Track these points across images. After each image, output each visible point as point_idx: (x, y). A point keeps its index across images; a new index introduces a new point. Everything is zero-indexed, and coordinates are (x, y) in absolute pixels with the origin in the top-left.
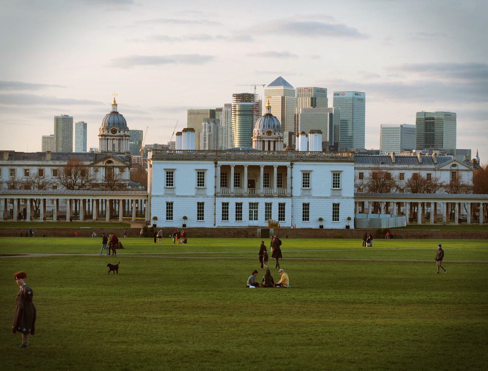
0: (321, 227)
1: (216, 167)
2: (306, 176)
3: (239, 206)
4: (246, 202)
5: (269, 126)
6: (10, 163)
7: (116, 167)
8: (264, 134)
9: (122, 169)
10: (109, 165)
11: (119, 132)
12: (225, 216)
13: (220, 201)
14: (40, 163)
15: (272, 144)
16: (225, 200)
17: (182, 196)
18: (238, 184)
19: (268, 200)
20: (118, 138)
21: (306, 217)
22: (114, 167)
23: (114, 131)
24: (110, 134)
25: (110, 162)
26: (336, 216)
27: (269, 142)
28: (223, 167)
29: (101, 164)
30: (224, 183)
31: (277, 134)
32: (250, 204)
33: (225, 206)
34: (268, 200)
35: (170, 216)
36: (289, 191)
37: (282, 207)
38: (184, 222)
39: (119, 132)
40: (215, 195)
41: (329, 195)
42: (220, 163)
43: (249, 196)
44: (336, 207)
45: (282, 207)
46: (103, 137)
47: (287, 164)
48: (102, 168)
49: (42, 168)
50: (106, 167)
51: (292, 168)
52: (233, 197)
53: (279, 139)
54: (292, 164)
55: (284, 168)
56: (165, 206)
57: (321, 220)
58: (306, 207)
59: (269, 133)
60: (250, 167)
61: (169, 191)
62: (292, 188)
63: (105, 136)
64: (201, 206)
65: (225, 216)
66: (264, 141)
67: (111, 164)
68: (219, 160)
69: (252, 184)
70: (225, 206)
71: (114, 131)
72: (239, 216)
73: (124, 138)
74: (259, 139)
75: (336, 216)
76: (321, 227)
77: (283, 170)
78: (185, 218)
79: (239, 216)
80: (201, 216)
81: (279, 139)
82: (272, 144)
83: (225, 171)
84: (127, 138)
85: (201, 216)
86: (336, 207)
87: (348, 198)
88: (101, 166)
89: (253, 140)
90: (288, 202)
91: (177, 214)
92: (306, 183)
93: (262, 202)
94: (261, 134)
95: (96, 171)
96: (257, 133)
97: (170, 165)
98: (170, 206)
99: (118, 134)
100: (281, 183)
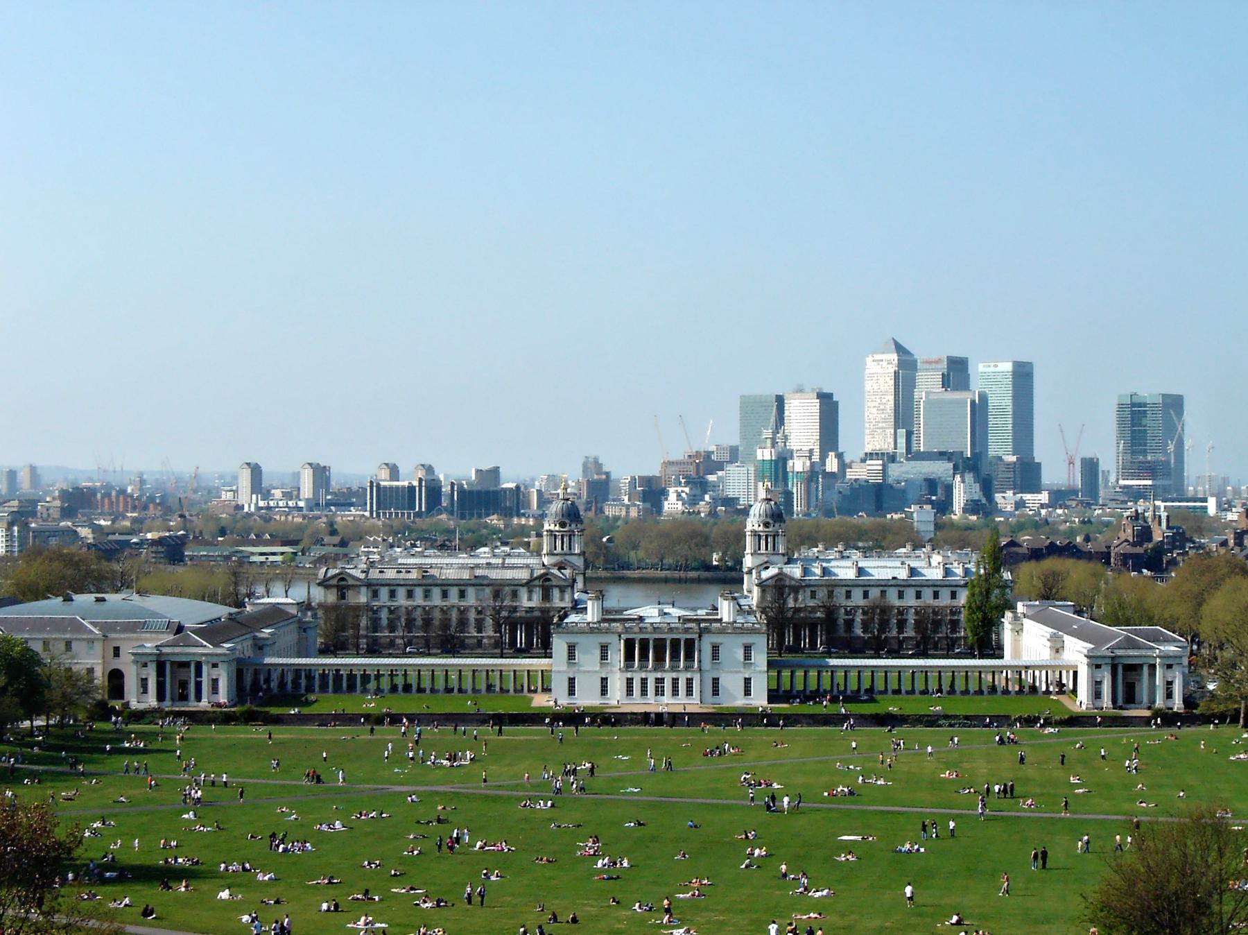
2: (715, 649)
3: (644, 682)
9: (562, 590)
16: (629, 675)
18: (644, 656)
19: (674, 675)
22: (552, 586)
23: (563, 525)
24: (557, 528)
25: (549, 580)
26: (747, 692)
29: (536, 582)
30: (629, 656)
33: (630, 682)
34: (674, 675)
35: (571, 692)
37: (689, 682)
44: (747, 681)
45: (689, 682)
55: (693, 640)
59: (766, 525)
65: (630, 691)
69: (659, 658)
70: (630, 682)
75: (747, 692)
77: (690, 644)
80: (604, 691)
83: (629, 645)
85: (604, 691)
86: (747, 681)
93: (668, 678)
95: (530, 592)
97: (572, 639)
98: (572, 682)
100: (689, 656)
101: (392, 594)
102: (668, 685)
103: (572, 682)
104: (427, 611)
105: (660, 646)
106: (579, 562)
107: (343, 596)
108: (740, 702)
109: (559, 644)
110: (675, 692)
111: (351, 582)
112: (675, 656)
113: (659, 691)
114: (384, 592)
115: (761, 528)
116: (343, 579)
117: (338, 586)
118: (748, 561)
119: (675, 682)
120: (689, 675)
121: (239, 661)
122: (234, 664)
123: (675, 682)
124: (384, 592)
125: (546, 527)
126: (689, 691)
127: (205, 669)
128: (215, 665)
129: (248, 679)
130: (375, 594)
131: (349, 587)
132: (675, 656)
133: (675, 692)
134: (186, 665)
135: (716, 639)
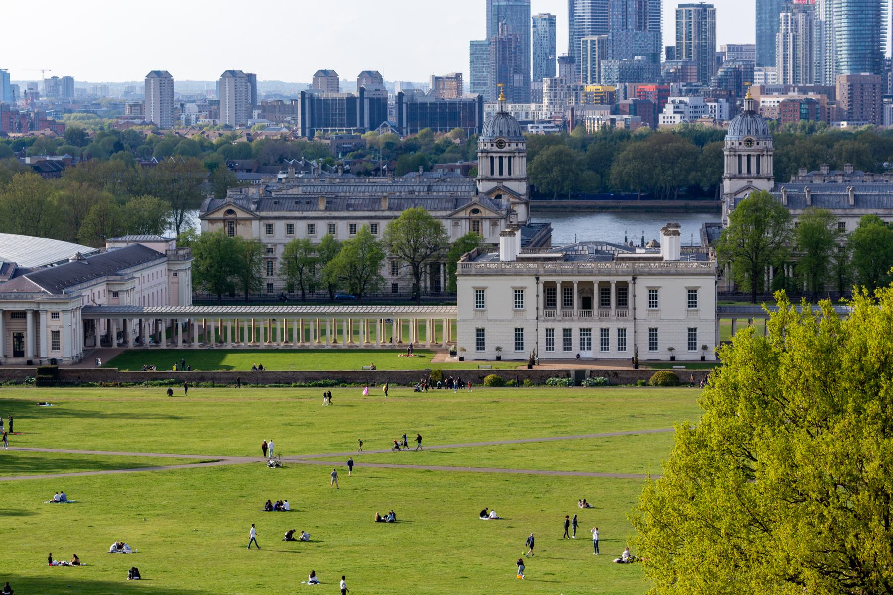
0: (673, 358)
1: (537, 283)
3: (567, 332)
4: (576, 327)
5: (749, 131)
6: (327, 214)
7: (486, 218)
8: (740, 144)
9: (494, 222)
10: (475, 215)
11: (509, 145)
12: (550, 345)
13: (543, 326)
14: (372, 214)
15: (753, 160)
16: (550, 325)
17: (496, 321)
18: (568, 302)
20: (508, 155)
21: (653, 345)
22: (482, 219)
24: (495, 148)
25: (476, 211)
27: (749, 157)
28: (546, 284)
29: (462, 214)
30: (550, 302)
31: (761, 144)
32: (581, 330)
33: (550, 332)
35: (480, 344)
36: (630, 312)
37: (622, 332)
38: (496, 353)
39: (509, 145)
40: (537, 319)
41: (682, 317)
42: (543, 279)
43: (579, 320)
44: (692, 332)
45: (622, 332)
46: (484, 154)
47: (629, 279)
48: (464, 221)
49: (374, 221)
50: (469, 218)
51: (634, 283)
52: (559, 321)
53: (765, 153)
54: (634, 279)
55: (625, 284)
56: (475, 333)
57: (671, 349)
58: (653, 332)
59: (749, 142)
60: (580, 283)
61: (479, 315)
62: (635, 309)
63: (487, 152)
64: (519, 332)
65: (550, 345)
66: (740, 156)
67: (478, 215)
68: (542, 275)
69: (587, 304)
70: (550, 332)
71: (500, 144)
72: (567, 346)
73: (517, 154)
74: (732, 153)
75: (692, 345)
76: (673, 358)
77: (623, 289)
78: (498, 349)
79: (567, 346)
80: (519, 345)
81: (765, 153)
82: (753, 160)
83: (549, 289)
84: (521, 154)
85: (519, 345)
86: (692, 332)
87: (707, 321)
88: (462, 218)
89: (726, 153)
90: (629, 327)
91: (490, 342)
92: (653, 300)
93: (596, 329)
94: (736, 144)
95: (456, 224)
96: (729, 143)
97: (480, 282)
98: (480, 333)
99: (507, 148)
100: (622, 301)
101: (290, 229)
102: (596, 337)
103: (480, 333)
104: (331, 248)
105: (586, 287)
106: (521, 188)
107: (232, 232)
108: (684, 354)
109: (465, 287)
110: (605, 345)
111: (240, 214)
112: (605, 301)
113: (586, 344)
114: (280, 227)
115: (743, 147)
116: (230, 212)
117: (224, 220)
118: (727, 186)
119: (605, 332)
120: (621, 325)
121: (86, 310)
122: (79, 314)
123: (605, 332)
124: (280, 227)
125: (481, 146)
126: (622, 346)
127: (43, 317)
128: (55, 315)
129: (101, 330)
130: (270, 229)
131: (237, 221)
132: (605, 301)
133: (605, 345)
134: (22, 315)
135: (653, 282)
